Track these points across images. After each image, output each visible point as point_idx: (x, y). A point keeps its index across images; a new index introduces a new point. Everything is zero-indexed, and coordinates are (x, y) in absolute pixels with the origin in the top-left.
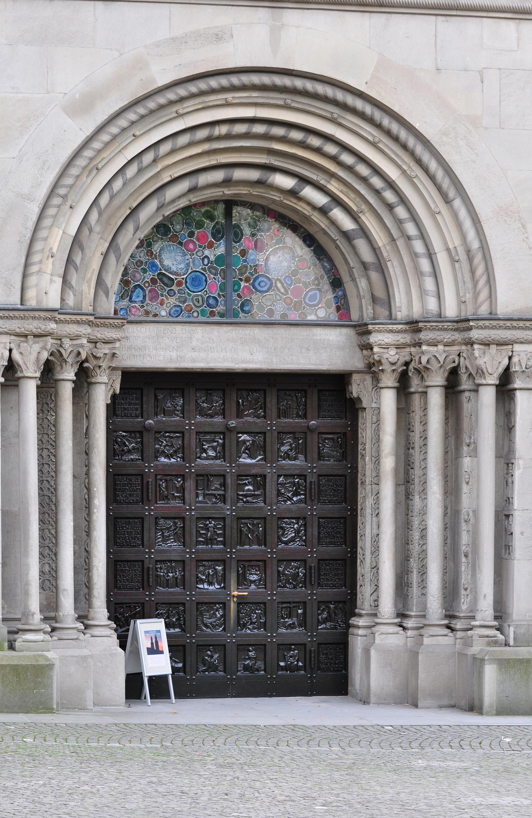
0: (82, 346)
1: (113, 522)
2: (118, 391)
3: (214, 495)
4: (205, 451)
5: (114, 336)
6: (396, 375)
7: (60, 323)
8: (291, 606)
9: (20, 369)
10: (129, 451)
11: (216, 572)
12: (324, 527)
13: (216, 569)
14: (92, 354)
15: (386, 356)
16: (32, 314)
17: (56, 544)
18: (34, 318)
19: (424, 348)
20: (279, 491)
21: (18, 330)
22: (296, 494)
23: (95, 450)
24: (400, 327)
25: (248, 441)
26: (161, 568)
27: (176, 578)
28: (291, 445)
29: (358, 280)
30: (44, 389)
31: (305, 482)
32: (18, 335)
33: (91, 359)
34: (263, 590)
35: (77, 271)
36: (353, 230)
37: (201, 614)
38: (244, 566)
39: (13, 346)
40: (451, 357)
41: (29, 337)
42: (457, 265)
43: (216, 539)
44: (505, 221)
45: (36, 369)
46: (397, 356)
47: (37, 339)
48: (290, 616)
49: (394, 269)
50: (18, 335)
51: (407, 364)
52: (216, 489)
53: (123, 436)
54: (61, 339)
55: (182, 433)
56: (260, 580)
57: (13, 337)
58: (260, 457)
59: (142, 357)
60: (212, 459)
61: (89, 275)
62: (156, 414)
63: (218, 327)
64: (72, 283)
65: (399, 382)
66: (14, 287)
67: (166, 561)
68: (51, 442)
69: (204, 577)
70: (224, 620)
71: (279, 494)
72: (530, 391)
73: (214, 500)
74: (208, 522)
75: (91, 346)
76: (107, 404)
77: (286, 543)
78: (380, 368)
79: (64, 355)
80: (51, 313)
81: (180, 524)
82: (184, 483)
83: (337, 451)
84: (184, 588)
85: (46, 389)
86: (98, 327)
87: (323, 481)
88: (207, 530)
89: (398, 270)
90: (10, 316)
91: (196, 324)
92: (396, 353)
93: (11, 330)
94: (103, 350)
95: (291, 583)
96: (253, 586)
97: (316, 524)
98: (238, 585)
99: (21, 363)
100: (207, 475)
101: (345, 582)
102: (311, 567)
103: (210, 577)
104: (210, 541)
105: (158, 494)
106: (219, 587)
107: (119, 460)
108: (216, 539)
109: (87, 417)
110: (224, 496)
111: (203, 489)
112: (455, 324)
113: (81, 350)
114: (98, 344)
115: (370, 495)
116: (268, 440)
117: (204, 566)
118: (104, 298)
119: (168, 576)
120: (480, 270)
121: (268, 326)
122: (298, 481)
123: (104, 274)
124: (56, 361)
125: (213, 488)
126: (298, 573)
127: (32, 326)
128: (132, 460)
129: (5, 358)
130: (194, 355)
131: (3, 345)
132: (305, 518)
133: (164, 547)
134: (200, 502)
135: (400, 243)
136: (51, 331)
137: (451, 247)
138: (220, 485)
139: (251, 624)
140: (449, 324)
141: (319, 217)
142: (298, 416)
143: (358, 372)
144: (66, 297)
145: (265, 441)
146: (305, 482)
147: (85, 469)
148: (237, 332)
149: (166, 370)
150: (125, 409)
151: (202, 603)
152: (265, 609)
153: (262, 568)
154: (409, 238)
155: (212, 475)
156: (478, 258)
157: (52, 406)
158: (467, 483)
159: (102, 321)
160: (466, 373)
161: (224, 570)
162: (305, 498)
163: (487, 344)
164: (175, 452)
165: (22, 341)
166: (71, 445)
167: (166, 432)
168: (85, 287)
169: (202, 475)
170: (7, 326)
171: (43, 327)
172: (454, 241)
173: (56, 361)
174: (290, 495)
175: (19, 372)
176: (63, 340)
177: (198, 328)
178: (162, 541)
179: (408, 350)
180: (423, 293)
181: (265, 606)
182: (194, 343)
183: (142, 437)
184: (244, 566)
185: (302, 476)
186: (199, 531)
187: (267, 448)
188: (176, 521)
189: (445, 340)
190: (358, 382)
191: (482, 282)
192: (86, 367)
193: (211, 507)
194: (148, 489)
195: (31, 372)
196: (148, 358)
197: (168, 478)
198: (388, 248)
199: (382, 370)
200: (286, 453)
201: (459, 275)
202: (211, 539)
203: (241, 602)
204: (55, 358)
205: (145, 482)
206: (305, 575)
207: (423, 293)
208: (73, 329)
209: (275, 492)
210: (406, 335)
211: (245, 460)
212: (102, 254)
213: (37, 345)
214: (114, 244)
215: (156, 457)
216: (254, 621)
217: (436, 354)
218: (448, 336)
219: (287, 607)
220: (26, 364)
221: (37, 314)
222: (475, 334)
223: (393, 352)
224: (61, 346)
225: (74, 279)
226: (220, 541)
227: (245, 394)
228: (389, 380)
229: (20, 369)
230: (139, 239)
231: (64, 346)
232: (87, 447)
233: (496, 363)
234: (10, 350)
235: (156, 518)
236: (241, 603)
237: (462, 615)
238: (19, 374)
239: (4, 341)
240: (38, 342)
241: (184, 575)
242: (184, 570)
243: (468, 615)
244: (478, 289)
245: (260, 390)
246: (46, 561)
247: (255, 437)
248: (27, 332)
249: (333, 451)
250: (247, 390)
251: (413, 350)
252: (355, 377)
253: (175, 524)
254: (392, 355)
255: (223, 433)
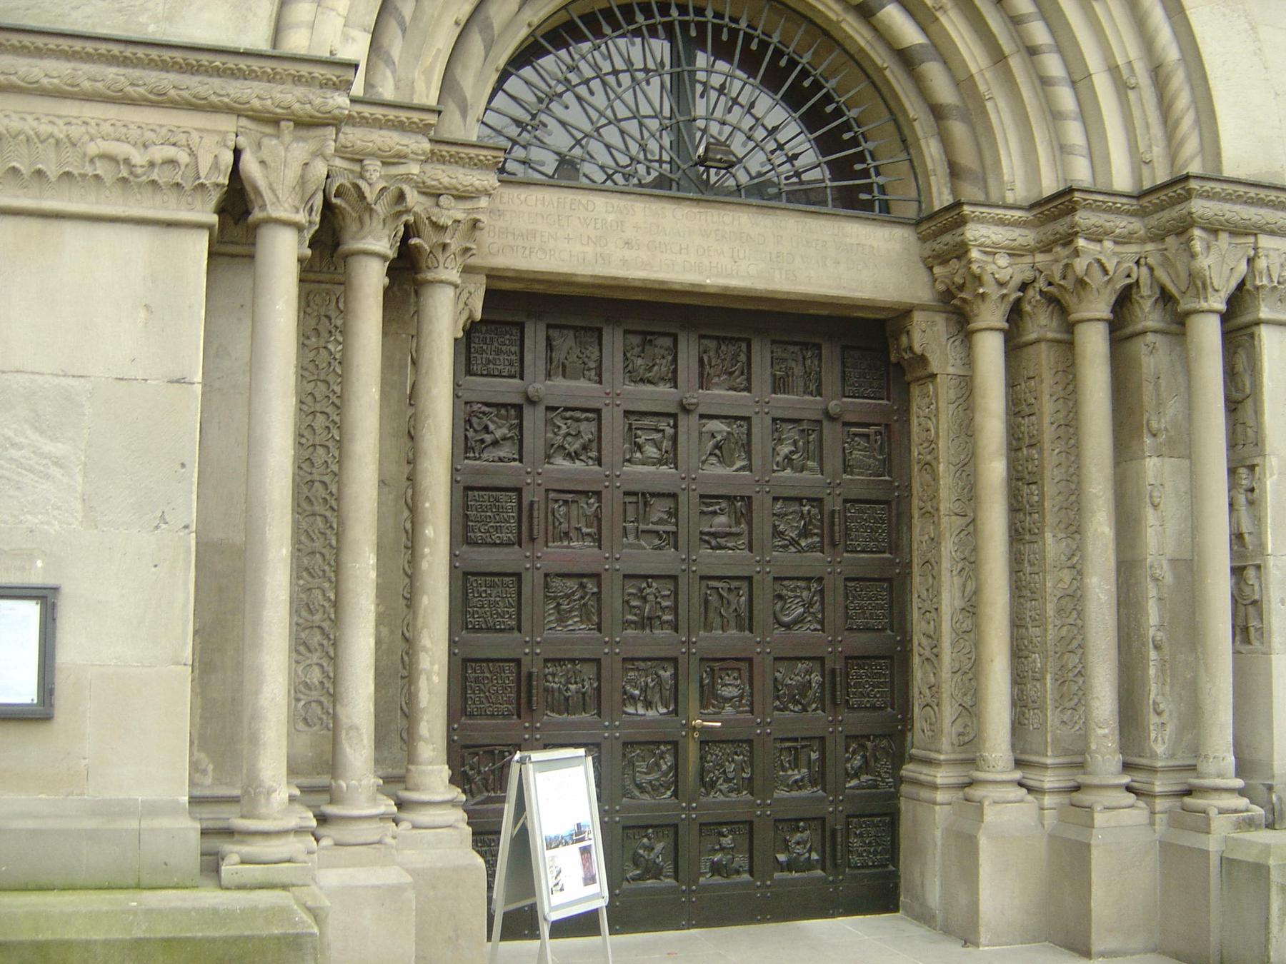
0: (407, 178)
1: (465, 581)
2: (478, 315)
3: (657, 532)
4: (639, 447)
5: (477, 183)
6: (1005, 308)
7: (362, 125)
8: (798, 745)
9: (260, 202)
10: (495, 443)
11: (660, 681)
12: (854, 597)
13: (659, 676)
14: (429, 218)
15: (991, 268)
16: (293, 68)
17: (337, 622)
18: (297, 80)
19: (1081, 242)
20: (775, 527)
21: (256, 103)
22: (805, 533)
23: (430, 421)
24: (1018, 214)
25: (720, 432)
26: (554, 675)
27: (584, 694)
28: (795, 443)
29: (923, 142)
30: (323, 286)
31: (821, 512)
32: (259, 117)
33: (427, 229)
34: (749, 716)
35: (404, 31)
36: (921, 45)
37: (631, 764)
38: (712, 670)
39: (242, 141)
40: (1126, 265)
41: (283, 124)
42: (1132, 95)
43: (659, 617)
44: (1224, 15)
45: (297, 203)
46: (1010, 270)
47: (303, 133)
48: (796, 766)
49: (1000, 113)
50: (259, 117)
51: (1024, 287)
52: (660, 522)
53: (484, 413)
54: (361, 161)
55: (598, 411)
56: (741, 697)
57: (244, 122)
58: (739, 464)
59: (527, 252)
60: (654, 464)
61: (430, 60)
62: (549, 375)
63: (674, 206)
64: (393, 53)
65: (1007, 321)
66: (255, 15)
67: (564, 660)
68: (334, 398)
69: (637, 692)
70: (676, 775)
71: (777, 533)
72: (1282, 328)
73: (657, 542)
74: (644, 585)
75: (428, 202)
76: (456, 340)
77: (787, 626)
78: (981, 291)
79: (367, 194)
80: (338, 71)
81: (591, 587)
82: (600, 507)
83: (874, 457)
84: (599, 715)
85: (328, 286)
86: (444, 163)
87: (853, 510)
88: (644, 599)
89: (1006, 116)
90: (239, 69)
91: (632, 197)
92: (1010, 265)
93: (241, 100)
94: (452, 212)
95: (799, 702)
96: (728, 709)
97: (841, 591)
98: (703, 706)
99: (262, 184)
100: (643, 494)
101: (893, 698)
102: (833, 671)
103: (649, 692)
104: (646, 622)
105: (550, 528)
106: (665, 711)
107: (476, 459)
108: (659, 617)
109: (414, 363)
110: (675, 534)
111: (637, 520)
112: (1134, 202)
113: (406, 188)
114: (443, 200)
115: (948, 535)
116: (754, 430)
117: (638, 669)
118: (457, 116)
119: (568, 689)
120: (1183, 100)
121: (766, 211)
122: (809, 511)
123: (458, 71)
124: (349, 209)
125: (655, 519)
126: (810, 682)
127: (290, 97)
128: (501, 460)
129: (223, 168)
130: (629, 254)
131: (217, 138)
132: (820, 580)
133: (560, 633)
134: (631, 546)
135: (1015, 63)
136: (336, 112)
137: (1120, 61)
138: (670, 514)
139: (727, 780)
140: (1125, 200)
141: (855, 24)
142: (807, 391)
143: (923, 308)
144: (377, 80)
145: (749, 434)
146: (821, 512)
147: (406, 470)
148: (709, 218)
149: (574, 279)
150: (489, 362)
151: (632, 744)
152: (751, 752)
153: (745, 674)
154: (1032, 51)
155: (653, 495)
156: (1178, 80)
157: (339, 323)
158: (1155, 506)
159: (453, 149)
160: (1150, 296)
161: (675, 676)
162: (822, 542)
163: (1213, 230)
164: (585, 448)
165: (266, 135)
166: (377, 397)
167: (566, 409)
168: (418, 77)
169: (635, 494)
170: (231, 91)
171: (318, 101)
172: (1127, 49)
173: (349, 209)
174: (793, 535)
175: (256, 209)
176: (366, 162)
177: (638, 204)
178: (557, 620)
179: (1028, 259)
180: (1062, 149)
181: (751, 747)
182: (629, 233)
183: (520, 417)
184: (712, 670)
185: (818, 502)
186: (628, 602)
187: (753, 447)
188: (585, 580)
189: (1118, 231)
190: (924, 325)
191: (1187, 122)
192: (416, 246)
193: (649, 558)
194: (531, 517)
195: (286, 210)
196: (540, 255)
197: (569, 497)
198: (988, 75)
199: (983, 296)
200: (786, 457)
201: (1137, 113)
202: (650, 619)
203: (708, 740)
204: (348, 202)
205: (525, 503)
206: (822, 685)
207: (1062, 149)
208: (391, 140)
209: (769, 529)
210: (1027, 232)
211: (716, 470)
212: (457, 23)
213: (301, 144)
214: (481, 17)
215: (548, 457)
216: (731, 775)
217: (1106, 255)
218: (1122, 224)
219: (789, 748)
220: (273, 191)
221: (304, 69)
222: (1199, 207)
223: (1003, 261)
224: (362, 177)
225: (395, 45)
226: (667, 622)
227: (712, 344)
228: (991, 315)
229: (260, 202)
230: (529, 25)
231: (368, 175)
232: (412, 423)
233: (1226, 269)
234: (237, 153)
235: (546, 575)
236: (707, 742)
237: (1159, 764)
238: (257, 214)
239: (223, 128)
240: (305, 140)
241: (599, 689)
242: (599, 679)
243: (1171, 763)
244: (1179, 136)
245: (739, 339)
246: (315, 660)
247: (729, 425)
248: (278, 110)
249: (869, 457)
250: (717, 338)
251: (1040, 258)
252: (918, 317)
253: (582, 586)
254: (1003, 268)
255: (674, 416)
